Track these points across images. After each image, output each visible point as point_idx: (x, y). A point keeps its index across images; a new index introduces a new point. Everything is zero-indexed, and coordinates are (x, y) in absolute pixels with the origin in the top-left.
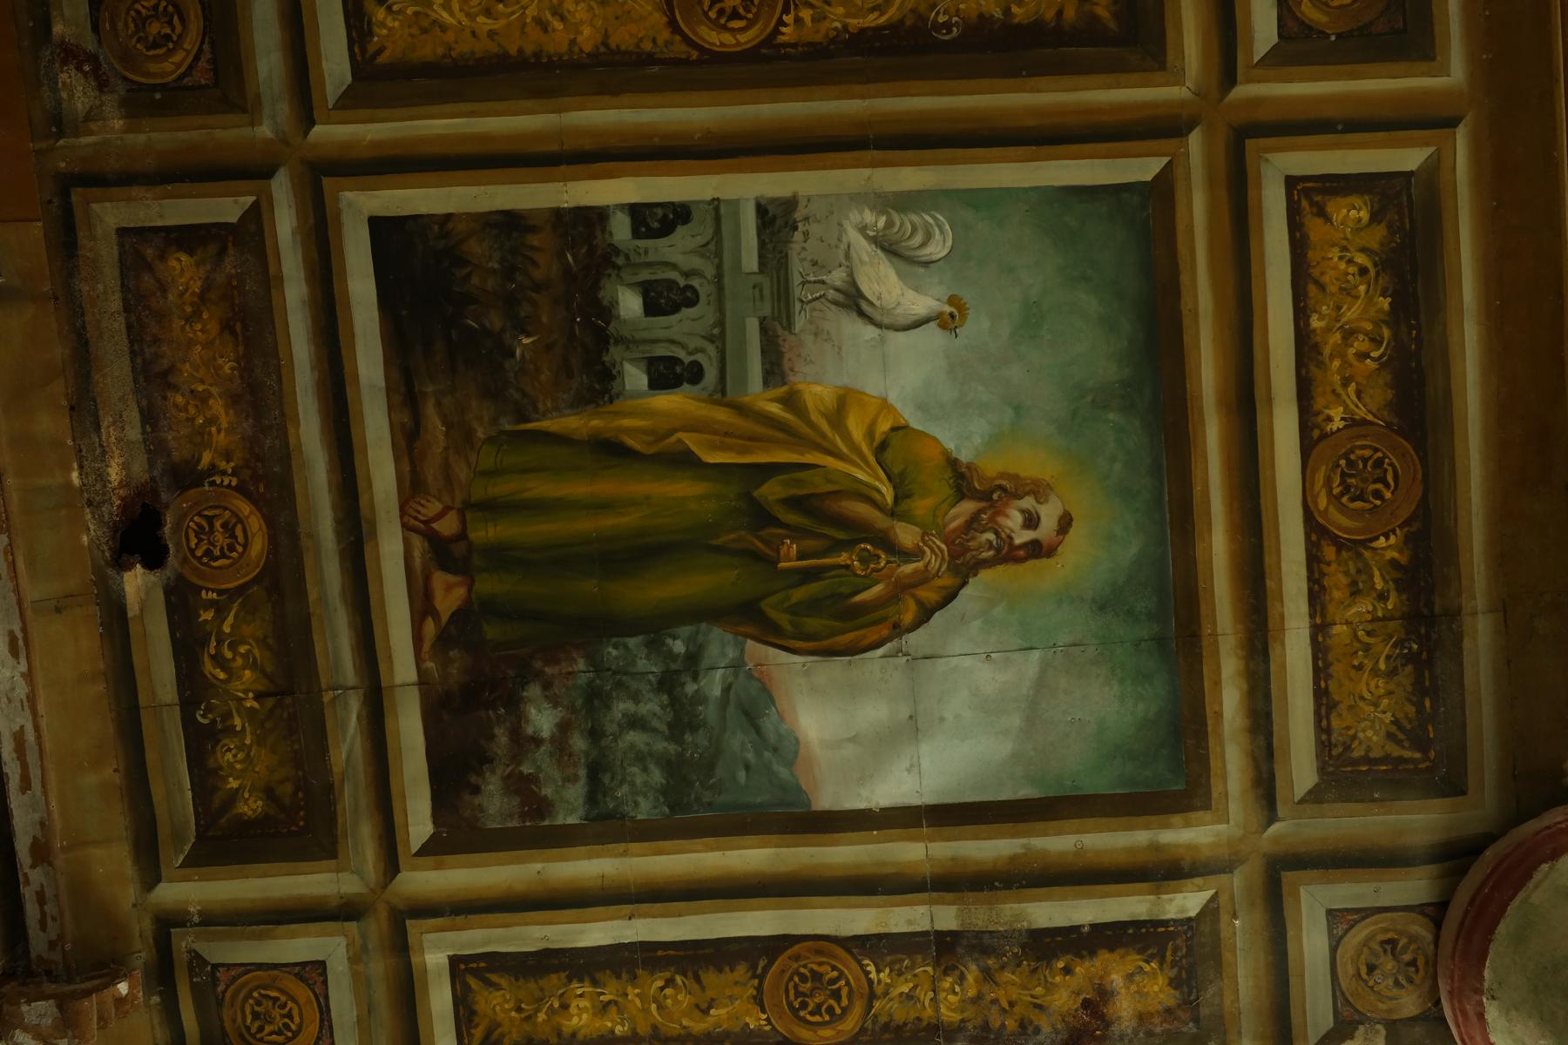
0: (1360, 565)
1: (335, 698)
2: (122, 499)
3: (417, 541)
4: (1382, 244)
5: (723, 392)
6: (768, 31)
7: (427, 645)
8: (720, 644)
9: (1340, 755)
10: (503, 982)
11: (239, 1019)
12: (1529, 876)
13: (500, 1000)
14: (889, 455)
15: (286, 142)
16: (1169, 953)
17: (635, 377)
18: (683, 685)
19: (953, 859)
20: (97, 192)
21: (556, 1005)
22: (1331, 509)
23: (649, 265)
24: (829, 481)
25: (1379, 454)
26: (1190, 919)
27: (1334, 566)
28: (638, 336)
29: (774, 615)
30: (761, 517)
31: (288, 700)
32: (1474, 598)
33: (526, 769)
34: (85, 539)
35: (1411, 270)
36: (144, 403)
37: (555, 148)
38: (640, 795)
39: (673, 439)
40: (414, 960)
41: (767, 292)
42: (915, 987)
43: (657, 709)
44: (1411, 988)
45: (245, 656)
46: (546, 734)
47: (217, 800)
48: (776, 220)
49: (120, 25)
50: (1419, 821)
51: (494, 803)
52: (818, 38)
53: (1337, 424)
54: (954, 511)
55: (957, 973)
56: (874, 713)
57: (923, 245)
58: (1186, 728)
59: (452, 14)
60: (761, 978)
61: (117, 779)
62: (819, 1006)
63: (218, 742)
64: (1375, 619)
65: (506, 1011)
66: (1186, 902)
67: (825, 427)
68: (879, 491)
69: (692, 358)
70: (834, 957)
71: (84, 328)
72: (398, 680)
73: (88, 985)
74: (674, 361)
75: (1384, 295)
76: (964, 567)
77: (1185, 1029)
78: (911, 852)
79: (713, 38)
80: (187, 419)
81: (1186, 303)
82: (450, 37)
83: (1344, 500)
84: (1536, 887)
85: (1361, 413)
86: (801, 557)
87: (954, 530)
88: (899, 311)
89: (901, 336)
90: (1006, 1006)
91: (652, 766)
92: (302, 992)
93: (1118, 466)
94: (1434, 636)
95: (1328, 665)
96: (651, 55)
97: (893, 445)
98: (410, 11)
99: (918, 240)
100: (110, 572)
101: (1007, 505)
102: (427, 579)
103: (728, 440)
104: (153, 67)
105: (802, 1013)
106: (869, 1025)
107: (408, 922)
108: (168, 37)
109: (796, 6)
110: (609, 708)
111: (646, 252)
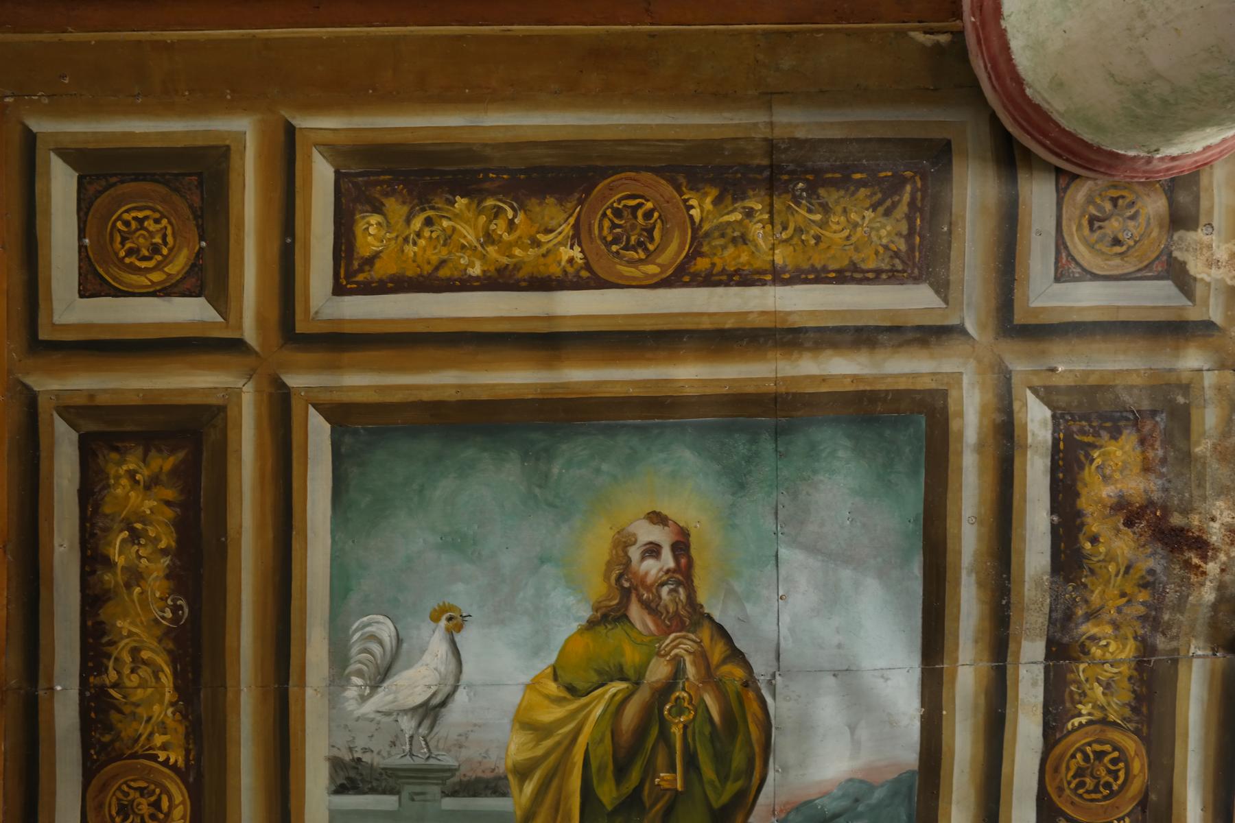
0: (717, 234)
4: (404, 203)
6: (172, 775)
9: (903, 262)
12: (1037, 108)
14: (580, 685)
16: (1086, 439)
19: (976, 642)
22: (659, 261)
24: (602, 740)
25: (609, 212)
26: (1054, 417)
27: (716, 260)
29: (725, 798)
32: (755, 125)
35: (429, 175)
41: (418, 789)
42: (1098, 681)
48: (351, 777)
50: (973, 191)
52: (181, 730)
53: (576, 253)
54: (638, 625)
55: (1087, 643)
56: (828, 709)
57: (381, 643)
58: (867, 411)
62: (1109, 772)
66: (1037, 420)
67: (549, 743)
68: (614, 695)
75: (452, 203)
76: (693, 617)
77: (1162, 426)
78: (967, 677)
81: (449, 396)
83: (651, 247)
84: (1048, 103)
85: (567, 229)
86: (672, 769)
87: (657, 625)
88: (442, 669)
89: (465, 668)
90: (1125, 600)
93: (605, 467)
94: (791, 167)
95: (813, 269)
97: (571, 682)
101: (635, 574)
105: (1115, 787)
109: (150, 748)
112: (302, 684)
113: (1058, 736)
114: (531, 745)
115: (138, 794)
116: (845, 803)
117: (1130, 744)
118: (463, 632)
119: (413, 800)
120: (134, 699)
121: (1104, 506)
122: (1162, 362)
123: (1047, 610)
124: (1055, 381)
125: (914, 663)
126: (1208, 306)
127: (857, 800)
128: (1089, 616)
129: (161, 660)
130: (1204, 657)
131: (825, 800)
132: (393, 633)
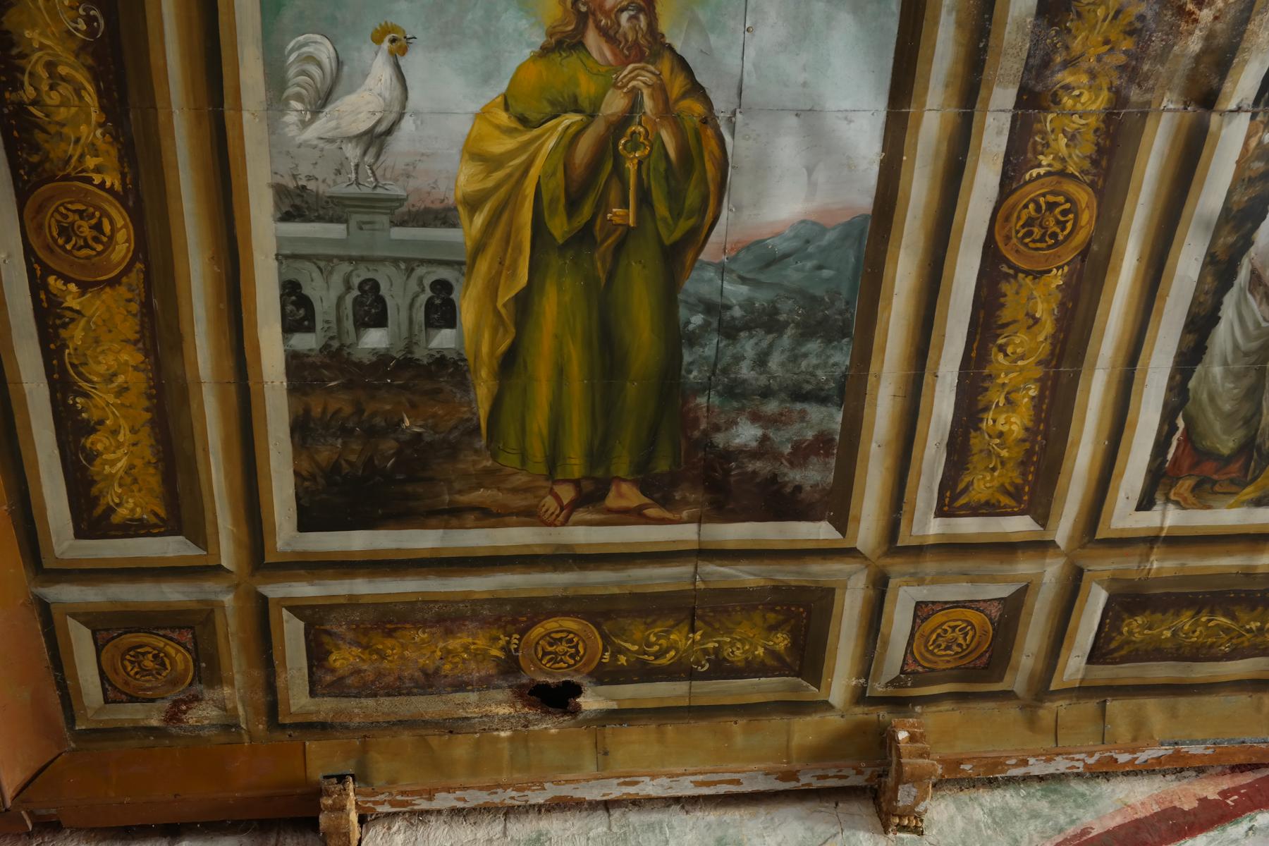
2: (524, 706)
3: (579, 515)
5: (461, 263)
6: (110, 198)
7: (668, 515)
8: (700, 283)
10: (967, 479)
13: (982, 483)
14: (533, 116)
15: (237, 586)
17: (444, 339)
18: (733, 318)
19: (947, 86)
20: (281, 708)
21: (998, 441)
23: (339, 320)
24: (554, 174)
28: (405, 334)
29: (677, 234)
30: (583, 238)
31: (699, 612)
33: (787, 449)
36: (449, 689)
37: (233, 388)
38: (826, 361)
39: (503, 311)
40: (931, 541)
41: (366, 218)
42: (1064, 131)
43: (752, 341)
45: (659, 638)
46: (759, 432)
47: (770, 662)
48: (296, 204)
49: (148, 685)
54: (595, 54)
55: (1060, 92)
56: (787, 149)
57: (320, 65)
59: (119, 460)
60: (1018, 270)
61: (742, 721)
62: (1058, 222)
63: (725, 659)
65: (992, 480)
68: (568, 127)
70: (1014, 207)
73: (894, 759)
74: (429, 305)
76: (654, 46)
78: (932, 123)
79: (122, 248)
82: (138, 462)
87: (615, 55)
88: (387, 95)
89: (411, 94)
90: (1107, 47)
91: (804, 350)
96: (142, 305)
98: (119, 491)
100: (581, 717)
102: (610, 511)
103: (507, 262)
104: (180, 666)
105: (1061, 238)
106: (1087, 179)
107: (899, 544)
108: (155, 656)
109: (83, 171)
110: (744, 381)
111: (327, 322)
112: (238, 108)
113: (1014, 186)
114: (481, 176)
115: (77, 217)
116: (795, 244)
117: (1083, 196)
118: (408, 56)
119: (361, 229)
120: (57, 119)
123: (1025, 55)
125: (880, 106)
128: (1066, 64)
129: (81, 77)
130: (1175, 110)
131: (777, 241)
132: (333, 55)
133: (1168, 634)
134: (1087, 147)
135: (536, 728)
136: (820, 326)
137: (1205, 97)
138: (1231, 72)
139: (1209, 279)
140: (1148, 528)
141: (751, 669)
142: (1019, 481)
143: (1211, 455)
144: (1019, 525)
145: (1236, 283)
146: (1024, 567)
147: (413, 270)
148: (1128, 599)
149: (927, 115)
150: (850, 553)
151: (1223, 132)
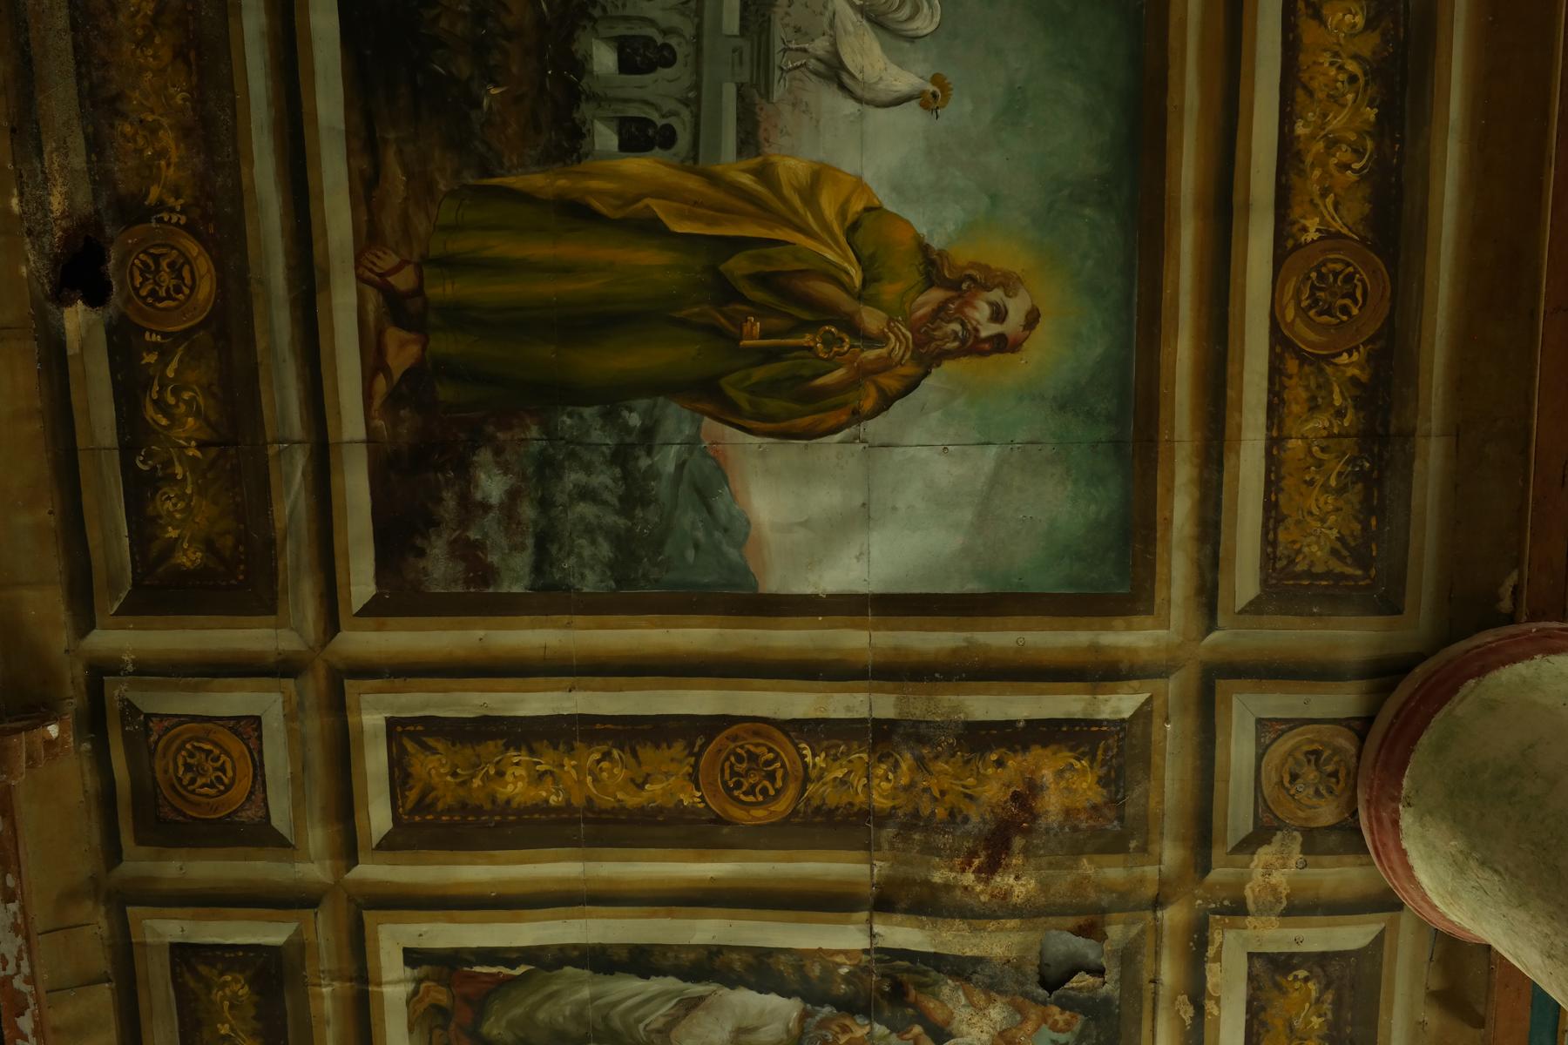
1: (280, 452)
2: (65, 230)
3: (372, 295)
4: (1374, 53)
5: (695, 159)
7: (377, 402)
8: (676, 420)
9: (1283, 568)
10: (440, 746)
11: (171, 770)
12: (1455, 691)
13: (436, 764)
14: (860, 236)
16: (1100, 752)
17: (605, 137)
18: (637, 458)
19: (896, 649)
21: (492, 772)
23: (626, 19)
25: (1351, 269)
26: (1123, 720)
27: (1295, 380)
29: (732, 393)
30: (726, 292)
31: (232, 451)
33: (473, 535)
34: (24, 270)
36: (90, 129)
39: (640, 205)
40: (351, 719)
41: (746, 57)
42: (850, 772)
43: (609, 482)
44: (1330, 798)
45: (188, 403)
50: (1353, 637)
51: (438, 567)
53: (1312, 235)
54: (921, 299)
55: (892, 760)
56: (826, 498)
57: (911, 18)
58: (1135, 532)
60: (698, 756)
61: (52, 521)
62: (753, 787)
63: (157, 489)
64: (1330, 436)
65: (440, 775)
66: (1121, 704)
67: (797, 201)
68: (848, 273)
69: (664, 121)
71: (27, 44)
72: (346, 437)
73: (19, 724)
74: (646, 123)
75: (1371, 105)
76: (928, 357)
78: (855, 640)
80: (135, 150)
83: (1312, 313)
84: (1462, 700)
85: (1337, 225)
86: (765, 335)
87: (920, 318)
88: (881, 86)
91: (600, 539)
92: (236, 746)
93: (1090, 263)
95: (1280, 478)
97: (864, 226)
99: (905, 12)
100: (51, 307)
102: (380, 333)
105: (736, 793)
107: (346, 682)
110: (560, 478)
117: (782, 806)
118: (919, 110)
121: (1033, 772)
122: (1170, 825)
124: (1157, 721)
125: (875, 587)
126: (1225, 866)
127: (726, 530)
132: (921, 33)
133: (224, 1029)
134: (833, 798)
135: (28, 247)
136: (629, 555)
137: (884, 902)
138: (913, 917)
139: (692, 956)
140: (379, 969)
141: (142, 525)
142: (440, 806)
143: (480, 1013)
144: (379, 817)
145: (689, 984)
146: (317, 837)
147: (687, 105)
148: (272, 973)
149: (865, 634)
150: (331, 623)
151: (851, 927)
